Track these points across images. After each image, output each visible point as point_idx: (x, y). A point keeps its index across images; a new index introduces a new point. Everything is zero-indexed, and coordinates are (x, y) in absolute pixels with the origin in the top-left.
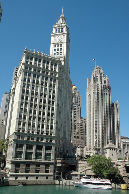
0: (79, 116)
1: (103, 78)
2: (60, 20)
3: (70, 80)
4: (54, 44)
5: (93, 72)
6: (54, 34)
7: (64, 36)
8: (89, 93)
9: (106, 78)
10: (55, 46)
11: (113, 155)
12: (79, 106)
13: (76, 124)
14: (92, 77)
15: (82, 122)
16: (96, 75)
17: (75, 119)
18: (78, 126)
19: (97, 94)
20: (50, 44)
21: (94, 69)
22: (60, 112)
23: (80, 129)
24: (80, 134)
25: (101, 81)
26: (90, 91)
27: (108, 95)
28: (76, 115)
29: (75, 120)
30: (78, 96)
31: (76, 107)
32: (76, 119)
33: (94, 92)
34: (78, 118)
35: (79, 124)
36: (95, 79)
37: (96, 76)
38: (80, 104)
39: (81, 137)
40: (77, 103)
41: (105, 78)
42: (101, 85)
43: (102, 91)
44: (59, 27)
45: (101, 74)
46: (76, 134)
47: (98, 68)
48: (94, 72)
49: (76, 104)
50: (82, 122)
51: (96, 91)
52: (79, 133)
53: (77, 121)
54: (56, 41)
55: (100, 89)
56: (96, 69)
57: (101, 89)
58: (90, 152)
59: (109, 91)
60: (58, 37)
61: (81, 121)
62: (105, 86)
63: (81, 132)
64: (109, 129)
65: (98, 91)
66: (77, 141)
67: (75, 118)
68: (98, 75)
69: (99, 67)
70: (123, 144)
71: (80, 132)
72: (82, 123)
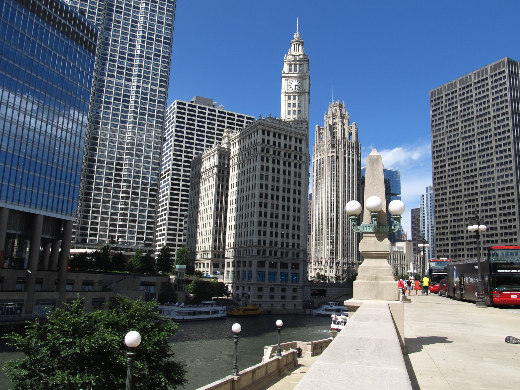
1: (346, 126)
4: (288, 93)
5: (327, 114)
6: (287, 75)
7: (304, 81)
8: (320, 155)
14: (326, 125)
16: (334, 121)
20: (280, 92)
25: (344, 134)
33: (330, 155)
36: (332, 128)
43: (345, 154)
44: (294, 61)
45: (342, 117)
47: (338, 105)
48: (330, 113)
51: (335, 154)
55: (341, 151)
58: (320, 267)
60: (294, 81)
62: (350, 144)
68: (338, 121)
69: (339, 104)
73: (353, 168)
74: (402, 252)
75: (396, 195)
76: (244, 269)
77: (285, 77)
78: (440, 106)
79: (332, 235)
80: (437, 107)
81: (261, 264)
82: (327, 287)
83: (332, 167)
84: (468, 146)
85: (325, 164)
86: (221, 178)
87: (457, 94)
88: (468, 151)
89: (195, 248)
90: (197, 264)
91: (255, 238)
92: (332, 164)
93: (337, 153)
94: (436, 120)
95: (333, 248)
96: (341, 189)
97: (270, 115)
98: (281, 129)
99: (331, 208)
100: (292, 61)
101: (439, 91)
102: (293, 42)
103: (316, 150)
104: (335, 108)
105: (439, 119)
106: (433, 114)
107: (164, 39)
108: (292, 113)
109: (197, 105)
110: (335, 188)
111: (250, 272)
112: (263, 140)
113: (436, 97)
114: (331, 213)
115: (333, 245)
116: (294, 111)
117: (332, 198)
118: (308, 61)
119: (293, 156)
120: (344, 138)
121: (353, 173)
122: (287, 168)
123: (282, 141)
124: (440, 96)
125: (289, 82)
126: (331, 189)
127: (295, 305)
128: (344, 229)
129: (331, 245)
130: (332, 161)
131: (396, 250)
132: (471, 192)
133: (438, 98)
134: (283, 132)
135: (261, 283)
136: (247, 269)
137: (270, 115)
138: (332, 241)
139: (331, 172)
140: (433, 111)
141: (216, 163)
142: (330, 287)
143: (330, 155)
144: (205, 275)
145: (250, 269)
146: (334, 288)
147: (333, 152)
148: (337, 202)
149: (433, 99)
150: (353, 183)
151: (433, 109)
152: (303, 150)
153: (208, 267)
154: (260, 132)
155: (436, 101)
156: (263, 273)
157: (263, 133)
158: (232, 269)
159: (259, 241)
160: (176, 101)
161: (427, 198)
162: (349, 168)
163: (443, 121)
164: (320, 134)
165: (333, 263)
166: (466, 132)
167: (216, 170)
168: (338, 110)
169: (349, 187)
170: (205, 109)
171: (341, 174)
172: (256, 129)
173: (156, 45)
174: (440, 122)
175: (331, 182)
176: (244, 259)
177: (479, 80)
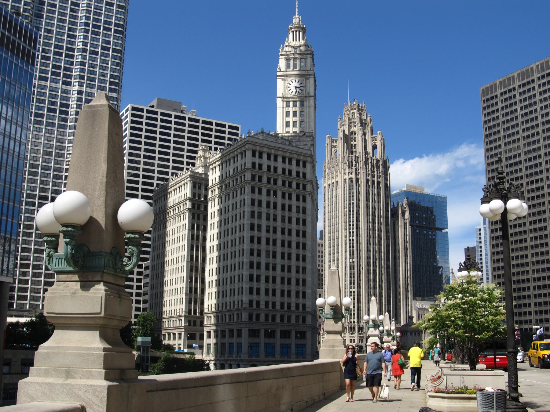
1: (368, 137)
2: (293, 32)
4: (286, 98)
5: (341, 119)
6: (284, 73)
7: (308, 81)
8: (333, 178)
10: (288, 102)
14: (340, 135)
16: (352, 129)
21: (345, 109)
36: (348, 139)
42: (364, 160)
43: (367, 175)
44: (293, 54)
45: (363, 124)
47: (356, 107)
48: (345, 118)
51: (353, 176)
54: (291, 91)
55: (362, 171)
60: (294, 81)
62: (375, 162)
64: (385, 276)
65: (358, 177)
68: (357, 129)
69: (358, 106)
75: (441, 229)
76: (231, 340)
77: (281, 76)
78: (494, 108)
79: (352, 290)
80: (490, 110)
81: (254, 333)
83: (349, 193)
84: (532, 163)
85: (340, 189)
86: (196, 216)
87: (517, 92)
88: (533, 170)
89: (161, 312)
90: (164, 335)
91: (245, 298)
92: (349, 190)
93: (357, 174)
94: (490, 128)
96: (363, 225)
97: (262, 129)
98: (277, 149)
99: (350, 251)
100: (291, 54)
101: (493, 88)
102: (291, 28)
103: (327, 170)
105: (494, 126)
107: (115, 26)
108: (291, 124)
109: (160, 111)
110: (355, 223)
111: (239, 344)
112: (254, 164)
113: (489, 96)
114: (350, 258)
116: (295, 122)
117: (351, 238)
118: (312, 54)
119: (294, 185)
120: (366, 153)
121: (379, 202)
122: (287, 202)
123: (280, 165)
124: (494, 95)
125: (287, 82)
126: (350, 225)
128: (369, 280)
130: (349, 186)
132: (538, 226)
133: (492, 98)
134: (280, 153)
135: (254, 358)
136: (235, 340)
137: (262, 129)
139: (350, 200)
140: (485, 115)
141: (189, 195)
143: (346, 177)
144: (176, 350)
145: (238, 340)
147: (352, 173)
148: (358, 242)
149: (485, 98)
150: (379, 216)
151: (486, 112)
152: (308, 176)
153: (180, 338)
154: (249, 154)
155: (489, 102)
156: (257, 345)
157: (254, 155)
158: (215, 341)
159: (251, 302)
160: (129, 106)
161: (485, 232)
162: (373, 194)
163: (498, 129)
164: (332, 147)
165: (354, 328)
167: (188, 205)
168: (357, 115)
169: (374, 222)
170: (170, 116)
171: (362, 204)
172: (243, 149)
173: (104, 35)
174: (496, 130)
175: (350, 215)
176: (231, 327)
177: (543, 74)
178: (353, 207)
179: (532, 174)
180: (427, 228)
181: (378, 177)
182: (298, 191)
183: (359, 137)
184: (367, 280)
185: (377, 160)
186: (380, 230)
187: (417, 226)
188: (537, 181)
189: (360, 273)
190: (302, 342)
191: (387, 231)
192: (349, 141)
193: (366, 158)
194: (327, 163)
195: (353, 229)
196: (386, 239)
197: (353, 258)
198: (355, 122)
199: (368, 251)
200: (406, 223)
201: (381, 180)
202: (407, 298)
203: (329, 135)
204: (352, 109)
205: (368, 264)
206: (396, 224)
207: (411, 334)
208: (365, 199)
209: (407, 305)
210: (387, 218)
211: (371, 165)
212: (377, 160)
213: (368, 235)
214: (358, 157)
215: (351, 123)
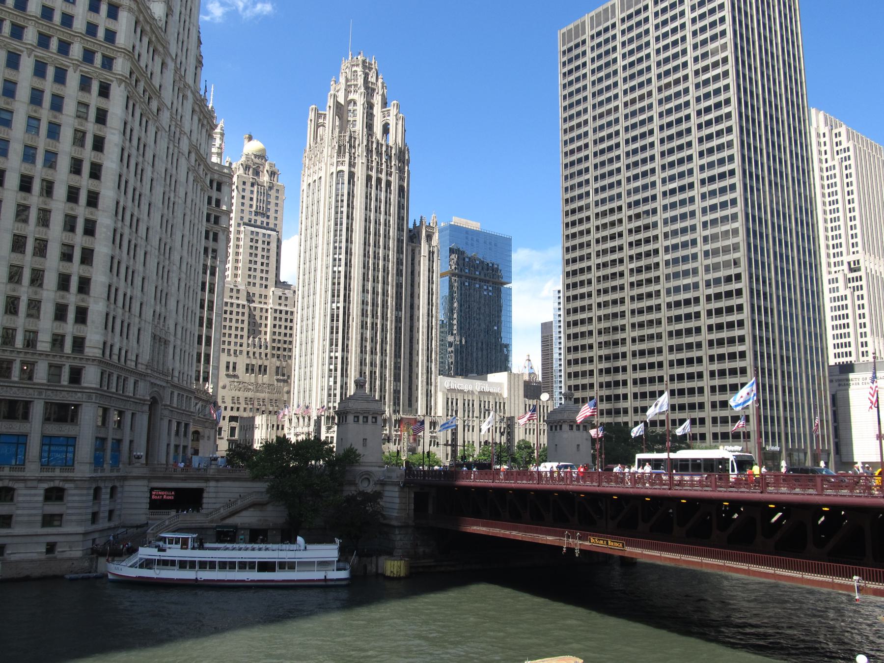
0: (272, 276)
1: (377, 110)
3: (200, 103)
9: (393, 111)
11: (365, 440)
12: (275, 230)
13: (258, 311)
14: (330, 102)
15: (283, 301)
17: (252, 290)
18: (266, 318)
19: (346, 182)
21: (343, 67)
22: (133, 249)
23: (274, 333)
24: (273, 355)
26: (317, 168)
27: (394, 187)
28: (258, 271)
29: (254, 294)
30: (271, 188)
31: (261, 235)
32: (257, 290)
33: (334, 169)
34: (266, 287)
35: (270, 311)
37: (351, 101)
38: (275, 225)
39: (278, 368)
40: (265, 220)
41: (386, 114)
42: (365, 143)
45: (369, 91)
46: (254, 353)
47: (360, 62)
48: (342, 80)
49: (259, 223)
50: (283, 301)
51: (345, 168)
52: (268, 351)
53: (263, 300)
55: (361, 161)
56: (349, 69)
57: (364, 160)
59: (401, 170)
61: (280, 298)
62: (384, 149)
63: (279, 349)
65: (352, 169)
66: (258, 387)
67: (254, 284)
68: (359, 98)
69: (364, 62)
70: (448, 399)
71: (273, 348)
72: (283, 308)
73: (388, 202)
74: (498, 395)
78: (580, 62)
80: (573, 66)
82: (207, 480)
84: (637, 145)
87: (617, 31)
88: (639, 157)
93: (352, 165)
95: (335, 383)
99: (333, 290)
104: (354, 69)
106: (566, 81)
110: (344, 245)
113: (572, 44)
115: (335, 378)
124: (580, 40)
126: (335, 248)
127: (51, 548)
128: (363, 339)
129: (330, 376)
131: (487, 389)
132: (643, 249)
138: (332, 367)
139: (337, 207)
142: (217, 480)
146: (228, 483)
148: (348, 276)
149: (565, 48)
150: (387, 236)
152: (122, 40)
164: (318, 126)
166: (633, 114)
175: (336, 231)
178: (341, 218)
179: (636, 164)
180: (481, 280)
181: (387, 174)
182: (86, 68)
183: (360, 109)
184: (359, 338)
185: (387, 146)
186: (386, 258)
187: (467, 277)
188: (645, 174)
189: (348, 328)
190: (66, 430)
191: (399, 262)
192: (345, 116)
193: (368, 141)
194: (308, 149)
195: (340, 254)
196: (397, 275)
197: (338, 302)
198: (355, 85)
199: (364, 291)
200: (433, 253)
201: (392, 179)
202: (428, 371)
203: (314, 106)
204: (353, 65)
205: (364, 313)
206: (417, 252)
207: (357, 418)
208: (363, 207)
209: (428, 382)
210: (400, 241)
211: (377, 152)
212: (387, 146)
213: (365, 266)
214: (355, 138)
215: (350, 86)
